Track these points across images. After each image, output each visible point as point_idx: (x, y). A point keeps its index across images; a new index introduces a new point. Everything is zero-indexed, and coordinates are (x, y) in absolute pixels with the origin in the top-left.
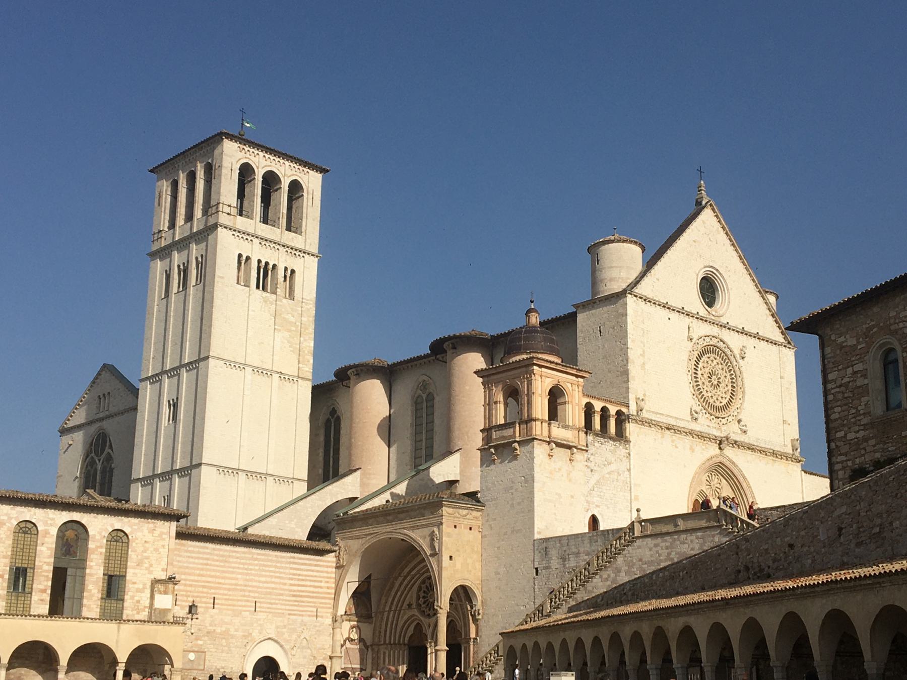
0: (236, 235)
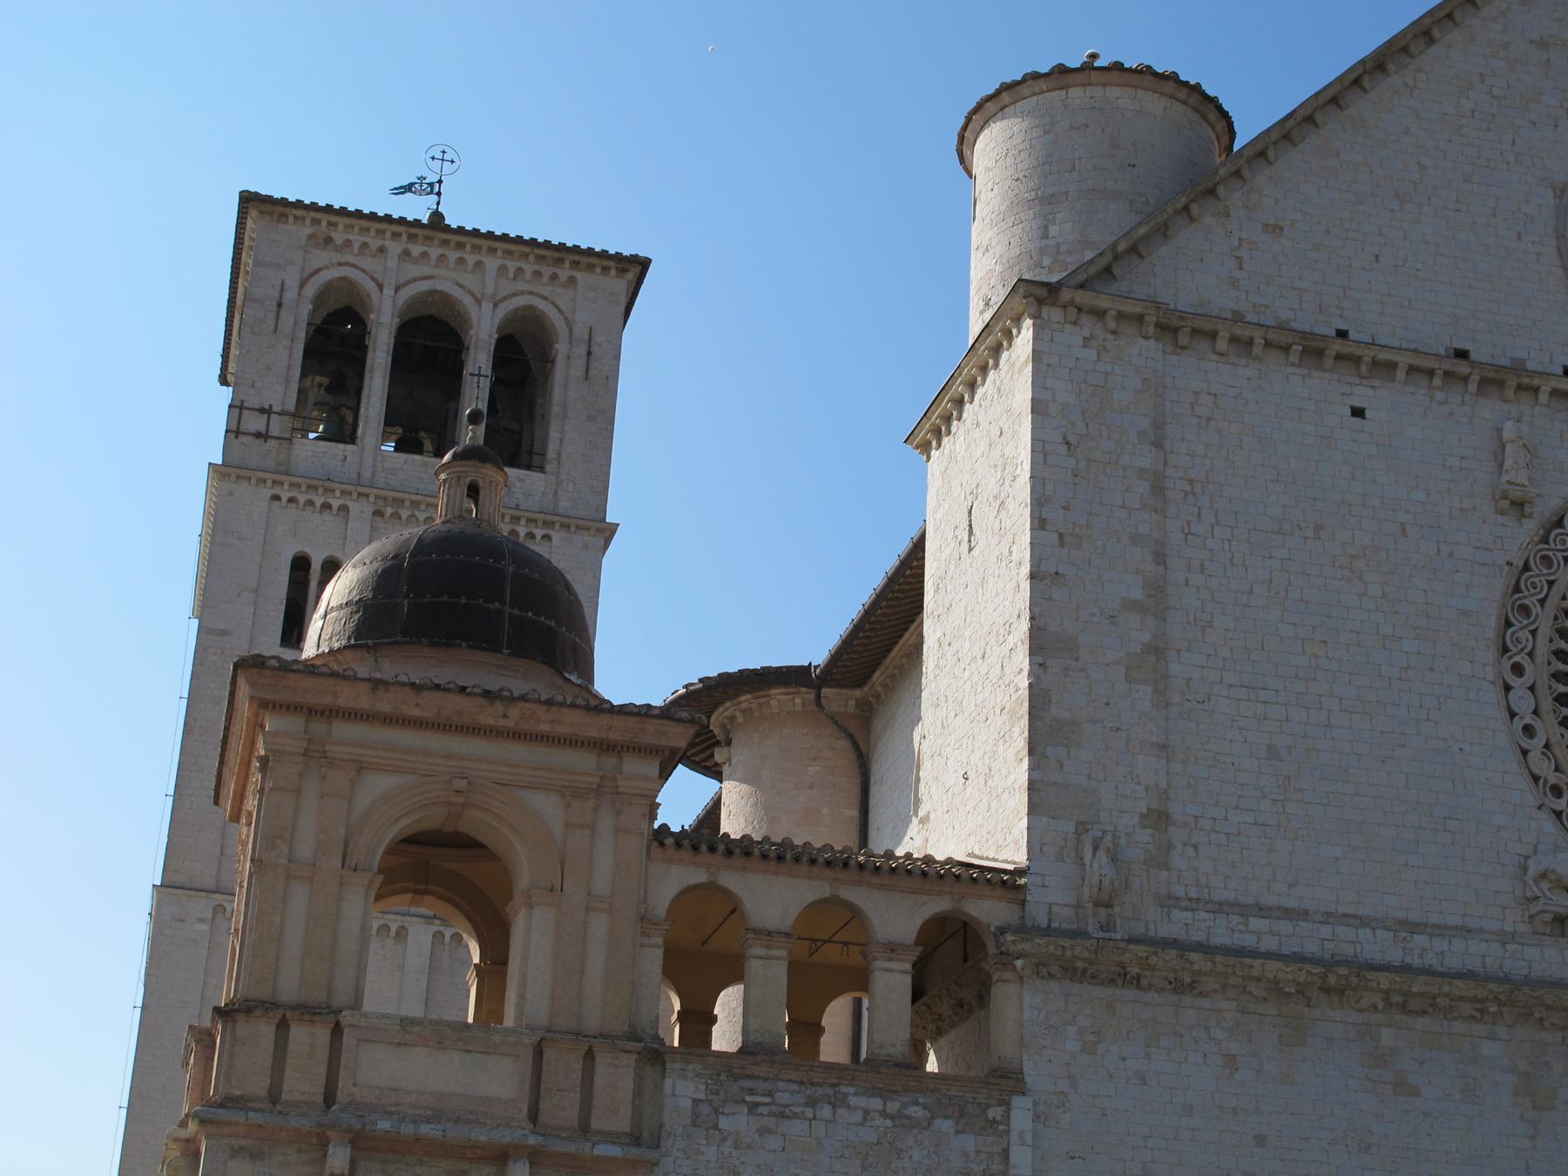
0: (284, 499)
